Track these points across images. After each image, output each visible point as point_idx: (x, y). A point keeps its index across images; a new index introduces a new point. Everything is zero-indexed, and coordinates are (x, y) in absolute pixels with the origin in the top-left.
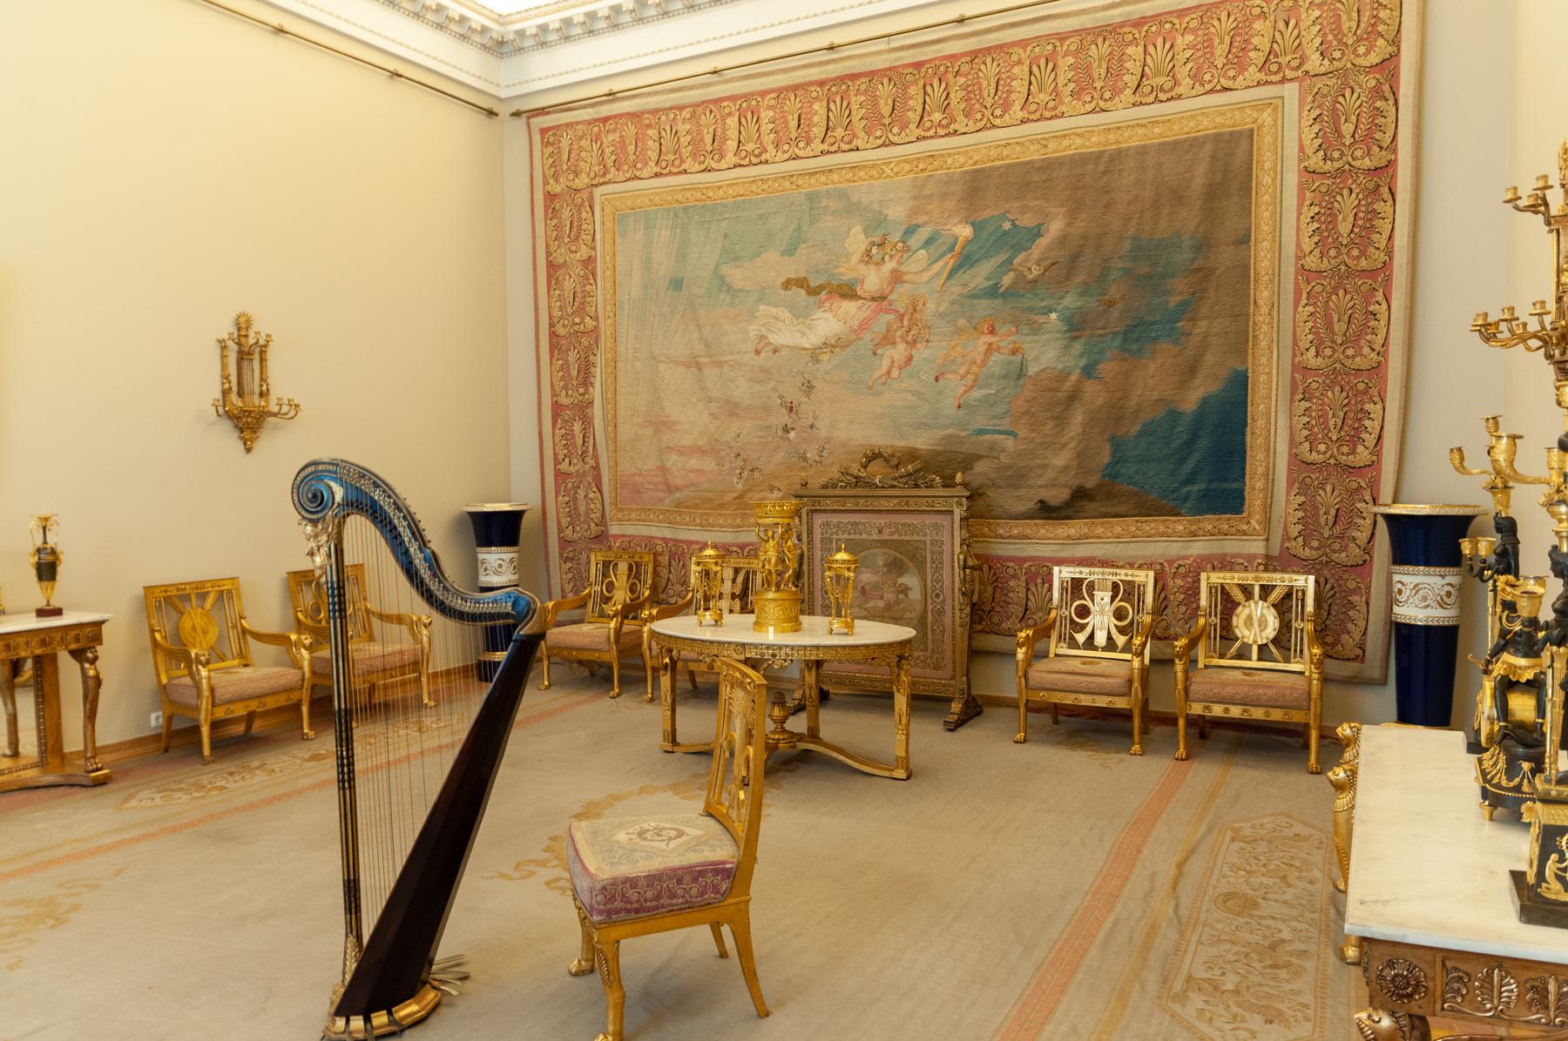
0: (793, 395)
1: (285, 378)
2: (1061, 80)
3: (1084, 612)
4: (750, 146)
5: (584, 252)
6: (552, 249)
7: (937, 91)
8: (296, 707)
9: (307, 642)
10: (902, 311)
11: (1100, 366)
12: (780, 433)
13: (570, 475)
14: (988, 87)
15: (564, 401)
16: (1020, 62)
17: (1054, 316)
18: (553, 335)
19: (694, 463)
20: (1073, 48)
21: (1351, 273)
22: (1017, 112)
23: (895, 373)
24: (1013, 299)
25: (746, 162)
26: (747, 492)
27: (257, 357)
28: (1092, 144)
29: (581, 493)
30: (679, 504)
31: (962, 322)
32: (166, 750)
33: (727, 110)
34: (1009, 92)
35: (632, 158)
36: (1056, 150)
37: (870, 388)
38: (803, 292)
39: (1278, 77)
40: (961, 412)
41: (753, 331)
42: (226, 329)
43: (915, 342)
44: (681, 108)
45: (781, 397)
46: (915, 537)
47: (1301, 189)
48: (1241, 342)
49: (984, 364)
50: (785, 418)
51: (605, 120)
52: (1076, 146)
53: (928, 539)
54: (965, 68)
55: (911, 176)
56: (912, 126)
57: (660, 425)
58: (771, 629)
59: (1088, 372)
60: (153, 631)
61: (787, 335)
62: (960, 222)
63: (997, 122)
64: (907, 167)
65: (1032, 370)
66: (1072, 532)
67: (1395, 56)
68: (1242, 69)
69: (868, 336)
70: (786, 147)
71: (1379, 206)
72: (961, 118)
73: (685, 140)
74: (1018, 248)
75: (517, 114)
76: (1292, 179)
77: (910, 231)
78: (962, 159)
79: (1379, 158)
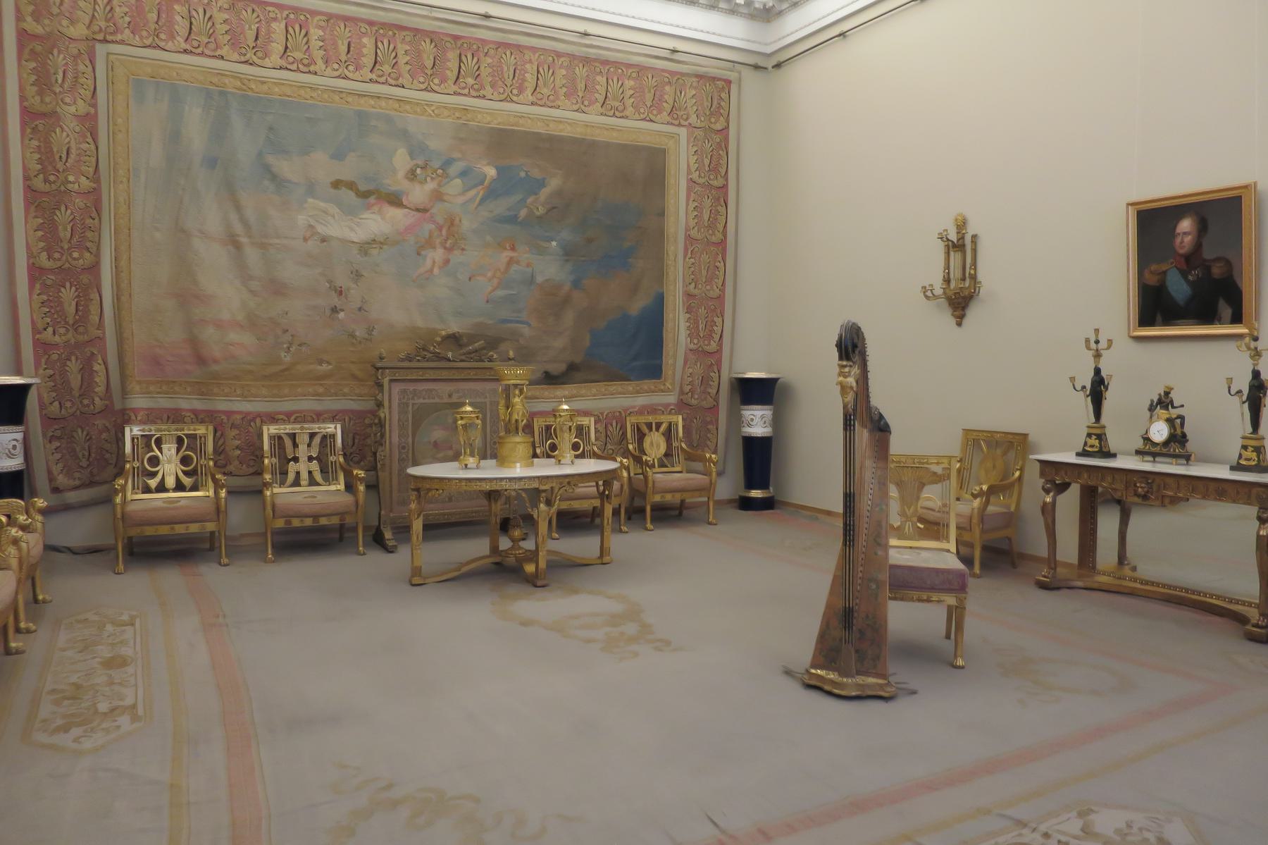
0: (342, 280)
2: (559, 83)
4: (298, 55)
5: (82, 107)
7: (470, 62)
12: (328, 312)
13: (56, 346)
17: (554, 243)
19: (233, 336)
21: (709, 243)
22: (528, 95)
23: (436, 271)
25: (294, 67)
28: (578, 132)
31: (488, 238)
35: (153, 26)
36: (555, 130)
38: (352, 194)
39: (676, 122)
41: (302, 219)
45: (330, 282)
47: (689, 190)
48: (660, 276)
50: (336, 301)
52: (567, 131)
54: (492, 52)
56: (451, 82)
57: (188, 296)
59: (576, 284)
62: (489, 164)
63: (515, 98)
64: (446, 113)
65: (539, 279)
67: (727, 127)
68: (660, 112)
70: (336, 66)
71: (719, 208)
72: (488, 87)
73: (222, 28)
76: (683, 184)
78: (489, 118)
79: (719, 182)
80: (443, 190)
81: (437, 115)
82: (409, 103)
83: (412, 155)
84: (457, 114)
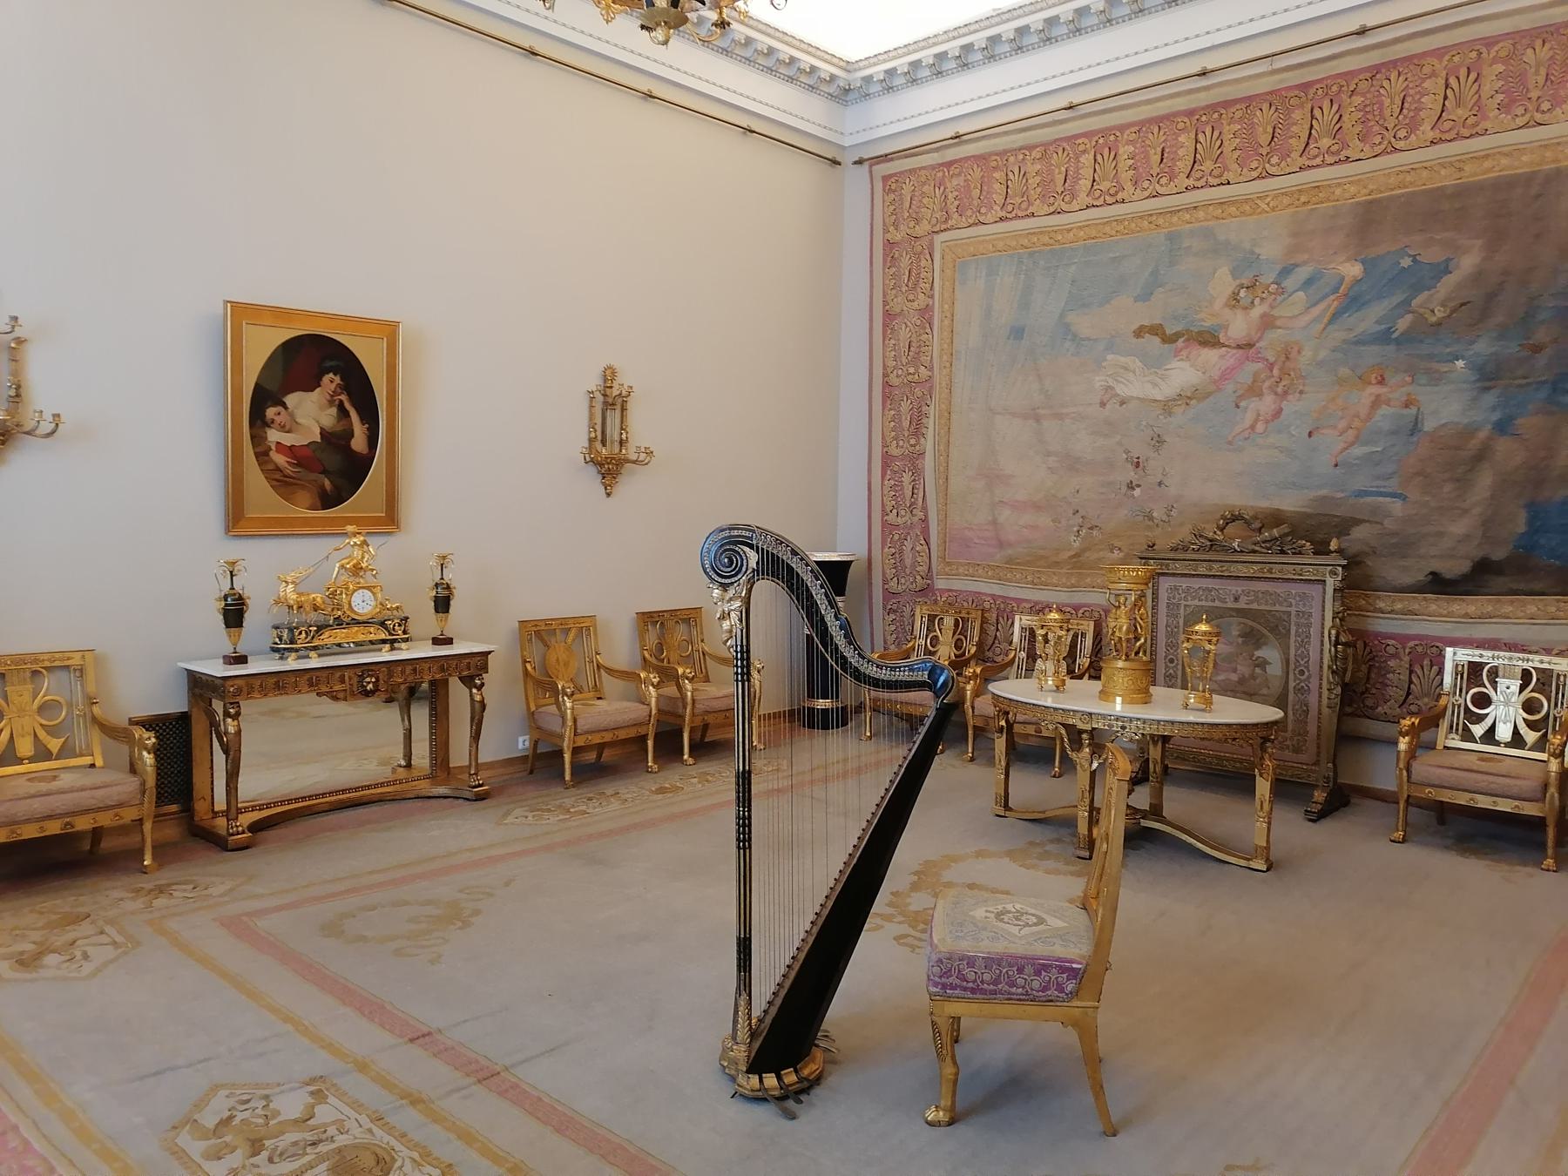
1: (643, 428)
2: (1487, 89)
3: (1483, 701)
4: (1105, 186)
5: (922, 300)
6: (889, 298)
7: (1328, 114)
8: (644, 738)
9: (656, 681)
10: (1272, 359)
11: (1518, 421)
12: (1124, 489)
14: (1391, 106)
15: (895, 451)
16: (1433, 74)
17: (1460, 363)
18: (886, 385)
20: (1503, 54)
22: (1426, 131)
23: (1260, 427)
24: (1414, 345)
26: (1084, 550)
27: (618, 407)
28: (1523, 165)
29: (908, 544)
30: (1010, 561)
31: (1344, 371)
32: (531, 772)
33: (1082, 148)
34: (1418, 110)
37: (1230, 443)
38: (1157, 340)
40: (1338, 471)
41: (1099, 381)
42: (594, 382)
43: (1286, 393)
44: (1031, 148)
45: (1127, 452)
46: (1277, 608)
49: (1369, 417)
50: (1131, 475)
51: (950, 164)
53: (1293, 610)
55: (1292, 210)
56: (1295, 155)
58: (1119, 699)
59: (1502, 427)
60: (525, 662)
61: (1136, 387)
62: (1348, 260)
63: (1401, 145)
64: (1286, 200)
65: (1429, 425)
66: (1471, 609)
69: (1229, 387)
70: (1146, 184)
73: (1034, 181)
74: (1417, 289)
75: (860, 162)
77: (1286, 271)
78: (1353, 189)
80: (1275, 313)
81: (1273, 209)
82: (1234, 202)
83: (1235, 273)
84: (1303, 199)
